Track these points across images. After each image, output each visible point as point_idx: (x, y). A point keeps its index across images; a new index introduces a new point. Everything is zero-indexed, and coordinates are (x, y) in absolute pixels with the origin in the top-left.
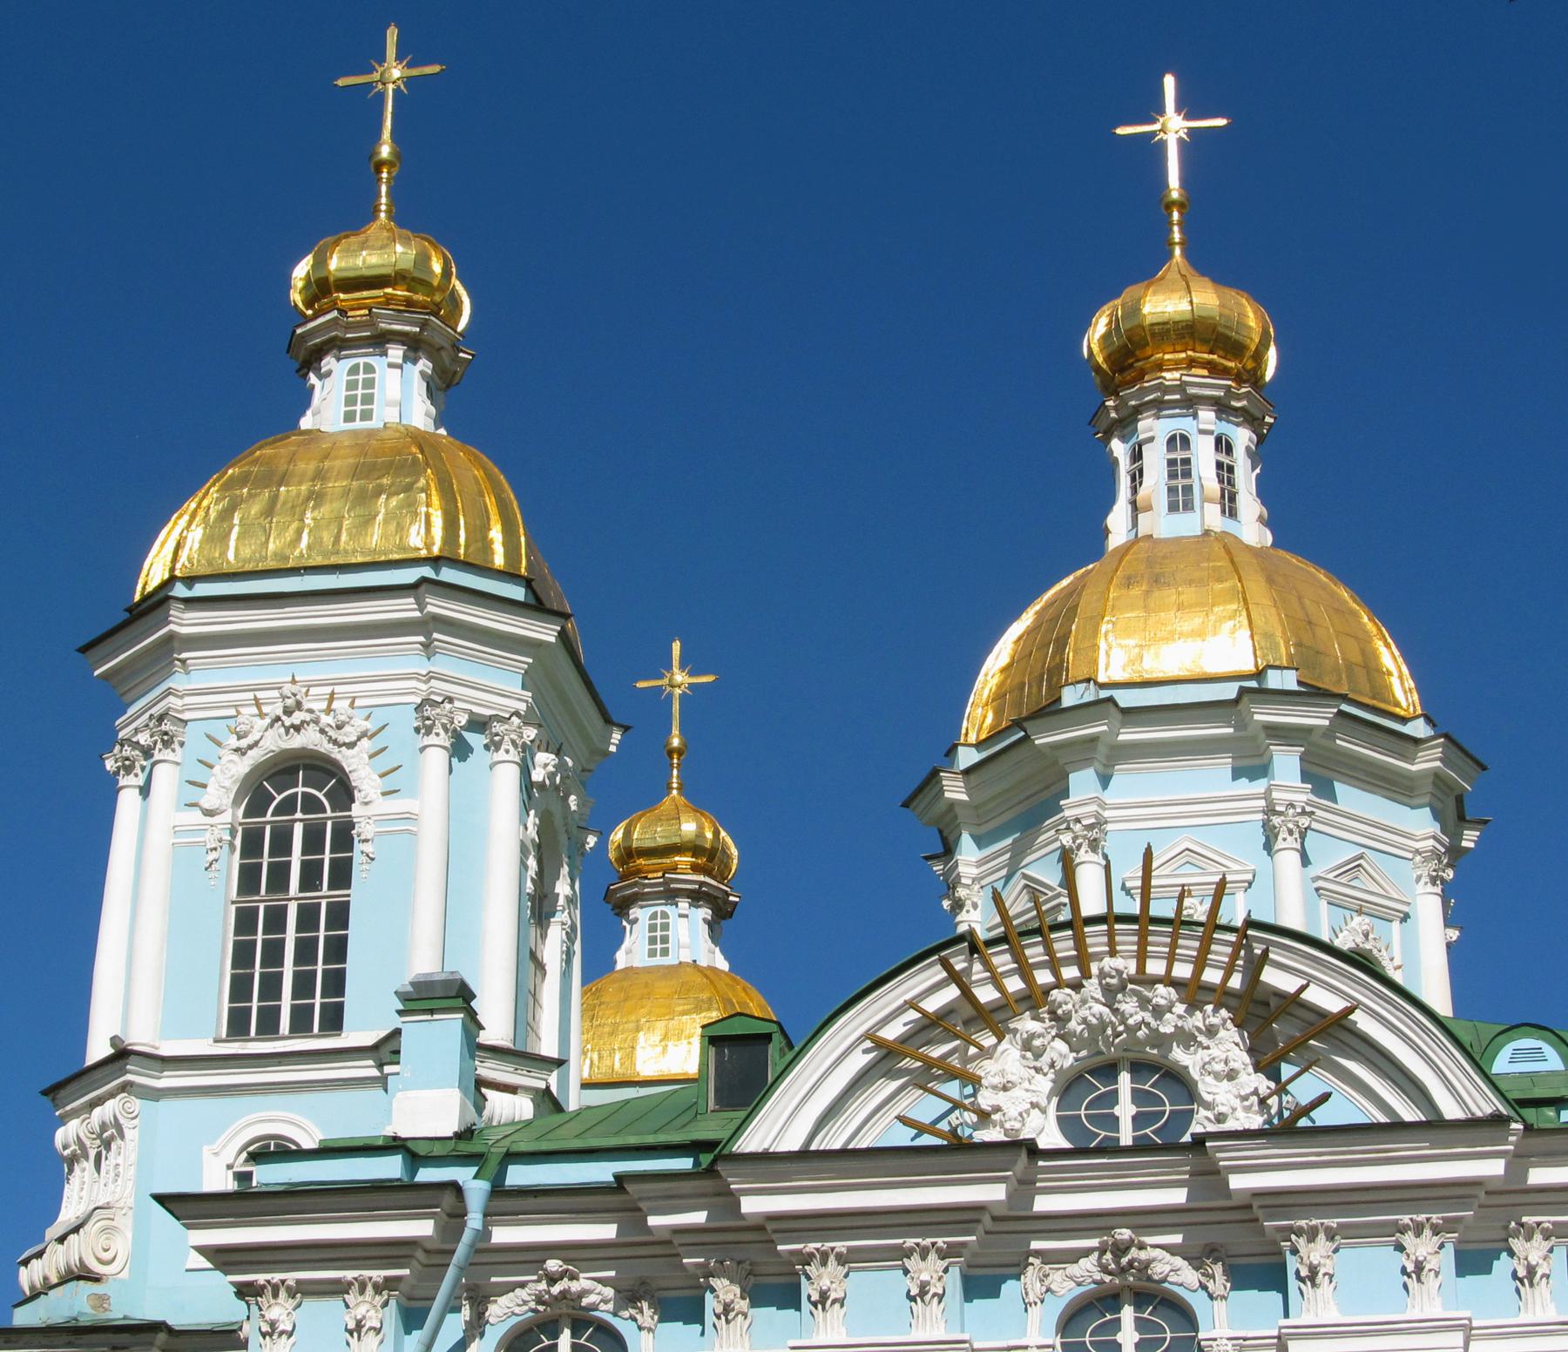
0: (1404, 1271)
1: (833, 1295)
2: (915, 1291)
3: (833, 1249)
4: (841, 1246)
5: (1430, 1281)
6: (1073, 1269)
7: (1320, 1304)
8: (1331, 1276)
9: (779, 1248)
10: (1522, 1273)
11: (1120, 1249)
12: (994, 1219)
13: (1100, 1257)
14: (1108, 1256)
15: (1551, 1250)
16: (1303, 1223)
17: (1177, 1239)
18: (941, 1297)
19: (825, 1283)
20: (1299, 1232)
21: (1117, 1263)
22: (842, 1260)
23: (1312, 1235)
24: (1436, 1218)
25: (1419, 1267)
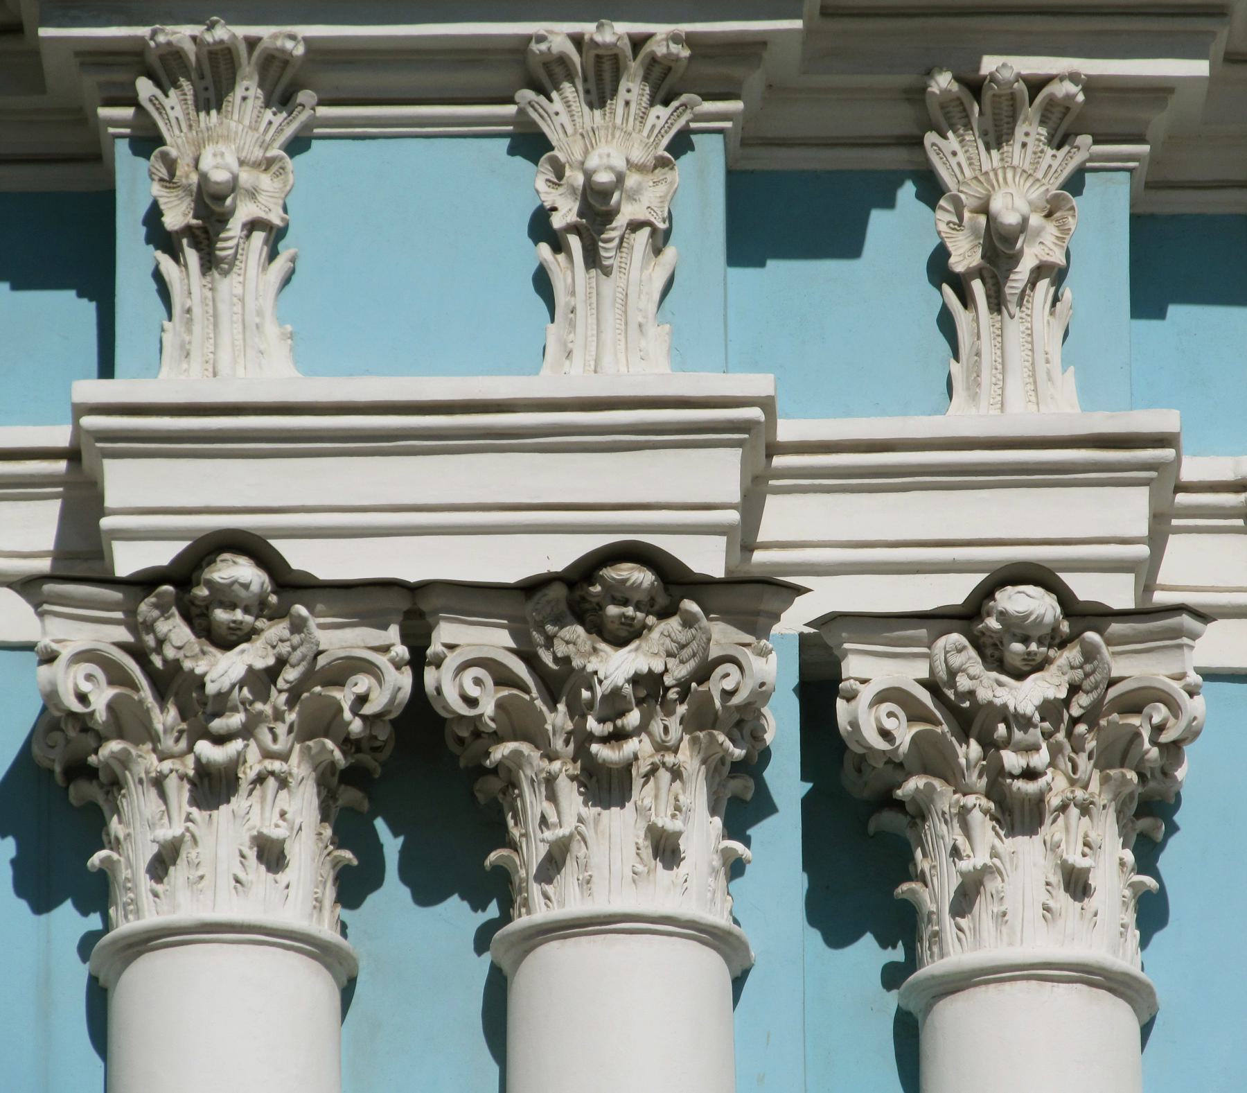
0: (540, 225)
5: (639, 271)
7: (230, 332)
8: (276, 235)
10: (964, 256)
15: (1075, 184)
16: (182, 34)
20: (167, 68)
23: (213, 80)
25: (597, 208)
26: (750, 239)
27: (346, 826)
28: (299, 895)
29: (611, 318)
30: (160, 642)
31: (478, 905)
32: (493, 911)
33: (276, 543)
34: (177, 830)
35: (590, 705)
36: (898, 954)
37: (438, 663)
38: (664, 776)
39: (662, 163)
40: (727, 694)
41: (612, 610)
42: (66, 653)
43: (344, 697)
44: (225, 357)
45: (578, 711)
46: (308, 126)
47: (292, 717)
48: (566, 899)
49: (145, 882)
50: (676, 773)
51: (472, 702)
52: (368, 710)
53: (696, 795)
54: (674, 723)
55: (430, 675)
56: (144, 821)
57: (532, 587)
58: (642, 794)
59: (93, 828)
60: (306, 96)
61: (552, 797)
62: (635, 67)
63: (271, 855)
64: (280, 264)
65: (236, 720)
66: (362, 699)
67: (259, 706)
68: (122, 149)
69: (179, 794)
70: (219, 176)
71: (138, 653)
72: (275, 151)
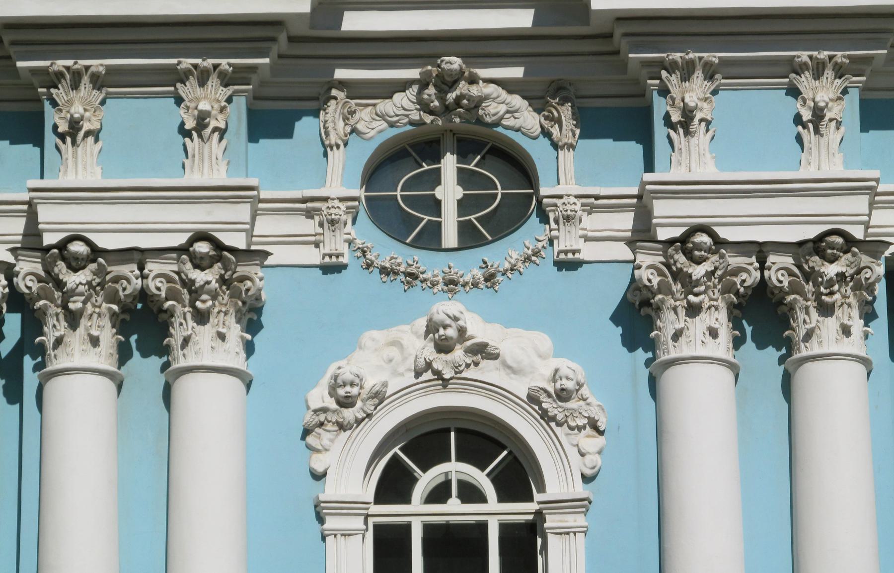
0: (798, 120)
1: (86, 126)
2: (190, 124)
3: (87, 68)
4: (98, 64)
5: (832, 135)
6: (385, 106)
7: (694, 156)
8: (708, 123)
9: (20, 64)
11: (446, 82)
12: (292, 39)
13: (420, 92)
14: (431, 90)
16: (677, 56)
17: (516, 72)
18: (222, 132)
19: (77, 110)
20: (671, 67)
21: (442, 99)
22: (98, 82)
23: (687, 72)
24: (840, 56)
26: (867, 124)
27: (735, 322)
28: (721, 347)
29: (824, 152)
30: (675, 262)
31: (779, 349)
32: (784, 351)
33: (715, 228)
34: (682, 325)
35: (822, 283)
36: (650, 355)
37: (769, 269)
38: (846, 306)
39: (839, 99)
40: (867, 279)
41: (829, 251)
42: (644, 266)
43: (737, 280)
44: (693, 165)
45: (817, 285)
46: (718, 86)
47: (719, 287)
48: (814, 348)
49: (671, 342)
50: (849, 306)
51: (781, 282)
52: (746, 284)
53: (855, 313)
54: (848, 289)
55: (766, 273)
56: (669, 322)
57: (801, 244)
58: (838, 312)
59: (650, 324)
60: (718, 76)
61: (807, 313)
62: (830, 66)
63: (713, 333)
64: (710, 133)
65: (702, 288)
66: (744, 281)
67: (709, 283)
68: (655, 93)
69: (682, 312)
70: (692, 104)
71: (668, 266)
72: (708, 95)
